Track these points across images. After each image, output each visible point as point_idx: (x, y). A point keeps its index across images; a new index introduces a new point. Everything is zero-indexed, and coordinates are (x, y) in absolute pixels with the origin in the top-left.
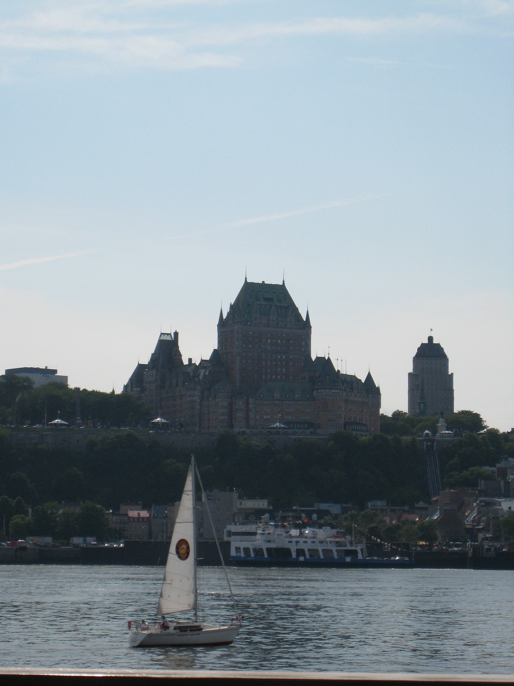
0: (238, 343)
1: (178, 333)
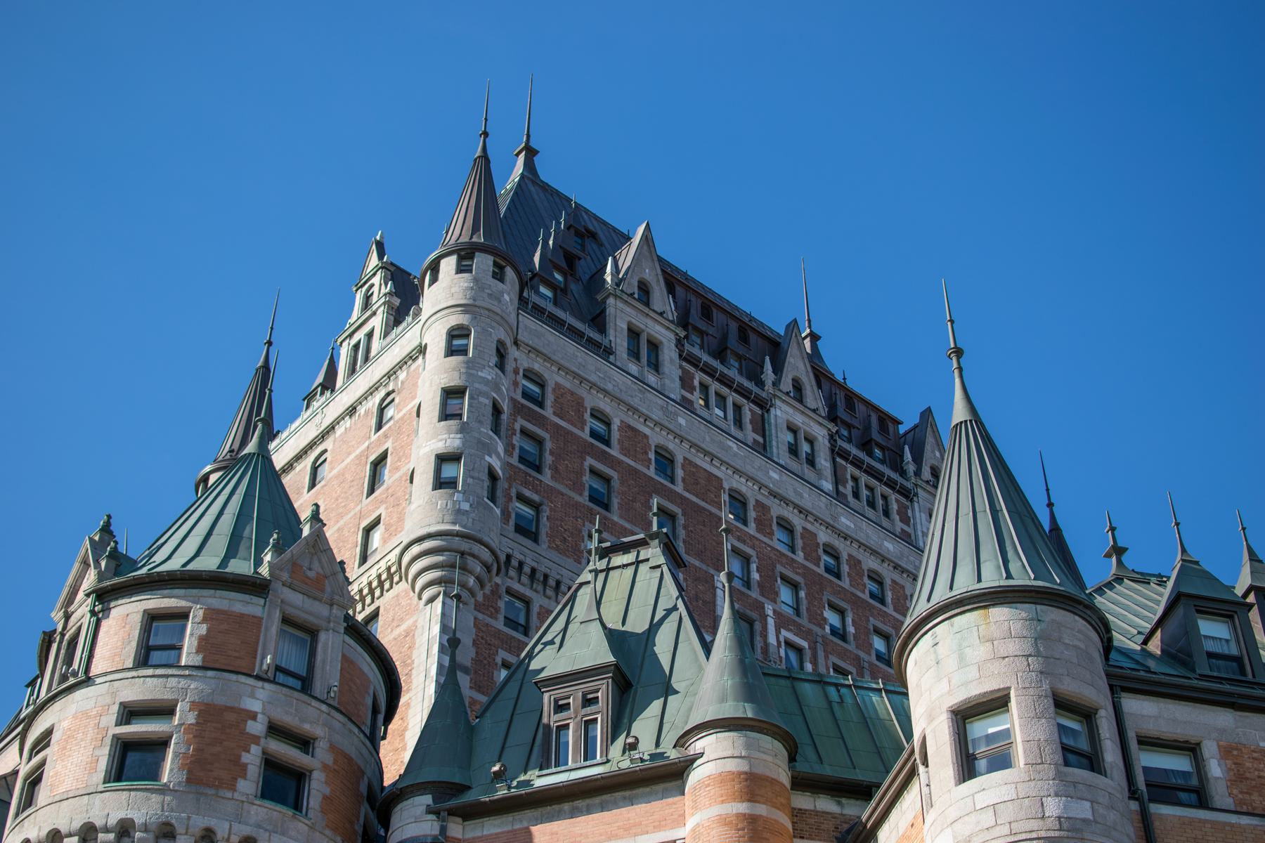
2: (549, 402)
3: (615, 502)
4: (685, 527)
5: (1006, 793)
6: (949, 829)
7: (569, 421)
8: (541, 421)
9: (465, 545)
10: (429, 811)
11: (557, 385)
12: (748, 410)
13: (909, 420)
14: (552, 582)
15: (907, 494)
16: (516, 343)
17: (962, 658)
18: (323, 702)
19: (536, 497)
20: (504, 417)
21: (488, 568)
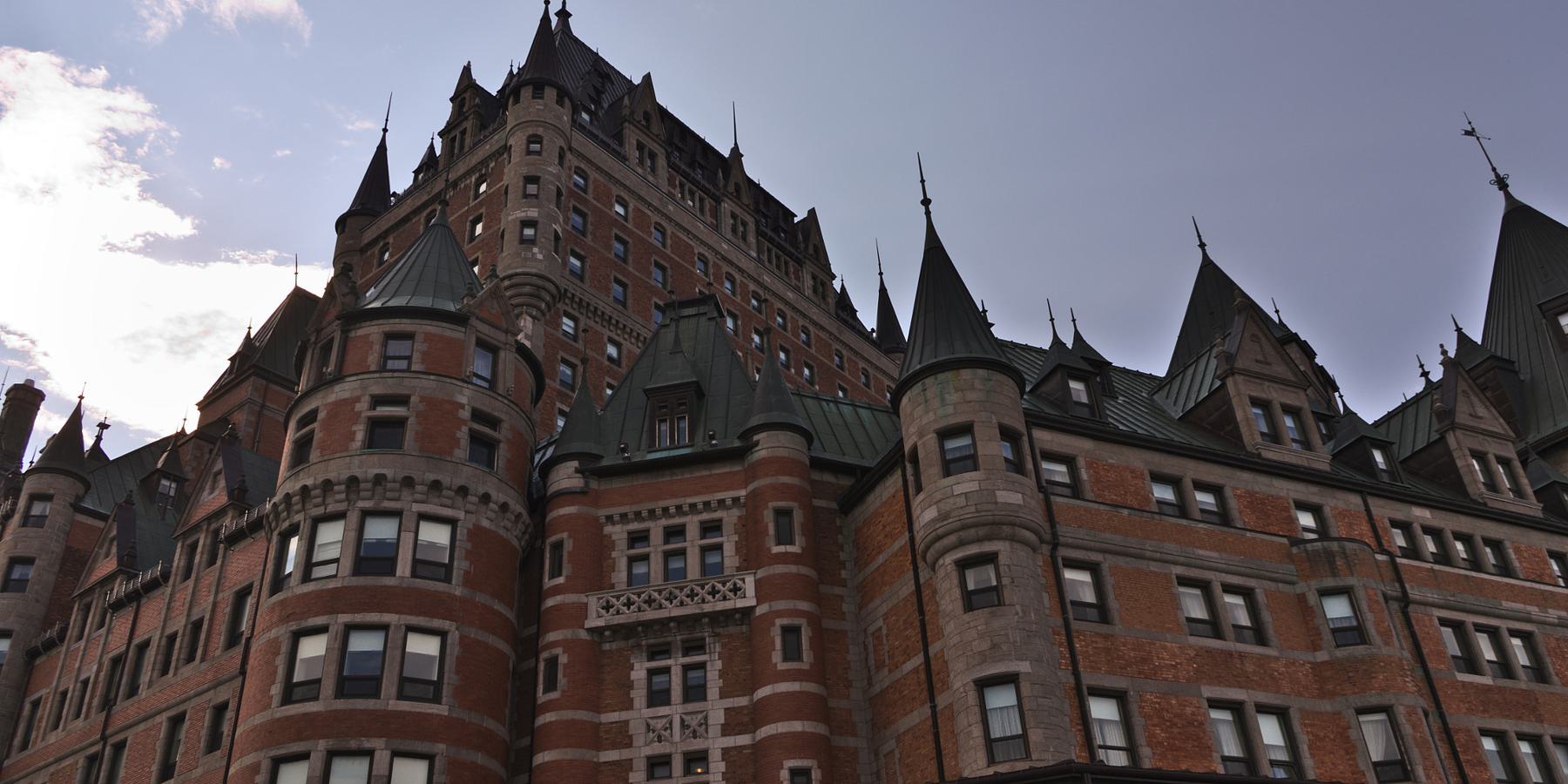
0: (533, 213)
1: (40, 396)
2: (590, 191)
3: (630, 259)
4: (672, 277)
5: (974, 486)
6: (935, 506)
7: (603, 204)
8: (585, 202)
9: (540, 282)
10: (577, 471)
11: (595, 180)
12: (708, 203)
13: (801, 215)
14: (592, 308)
15: (800, 263)
16: (570, 149)
17: (943, 399)
18: (505, 398)
19: (582, 253)
20: (563, 198)
21: (553, 296)
